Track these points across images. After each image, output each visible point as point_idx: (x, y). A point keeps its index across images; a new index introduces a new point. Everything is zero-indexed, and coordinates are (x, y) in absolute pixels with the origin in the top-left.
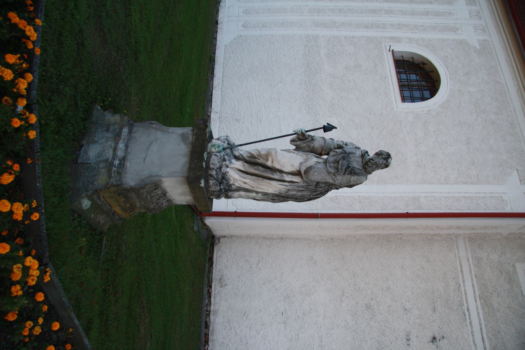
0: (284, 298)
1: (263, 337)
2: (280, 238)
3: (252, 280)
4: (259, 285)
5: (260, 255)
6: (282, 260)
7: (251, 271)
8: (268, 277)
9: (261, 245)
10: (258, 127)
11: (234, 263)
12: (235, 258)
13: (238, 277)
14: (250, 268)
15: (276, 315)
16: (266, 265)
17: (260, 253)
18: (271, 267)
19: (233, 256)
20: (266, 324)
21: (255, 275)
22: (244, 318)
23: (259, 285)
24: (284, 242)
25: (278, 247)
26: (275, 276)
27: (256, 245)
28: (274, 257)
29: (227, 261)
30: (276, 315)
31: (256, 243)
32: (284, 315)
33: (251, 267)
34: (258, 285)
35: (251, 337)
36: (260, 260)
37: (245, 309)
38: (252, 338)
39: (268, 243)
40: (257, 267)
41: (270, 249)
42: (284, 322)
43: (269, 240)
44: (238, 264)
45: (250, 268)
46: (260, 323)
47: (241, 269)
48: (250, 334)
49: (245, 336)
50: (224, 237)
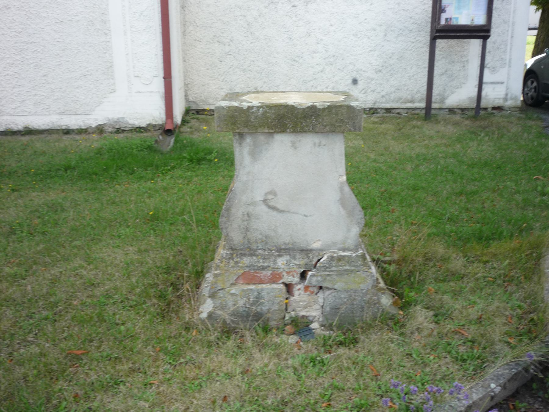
0: (272, 4)
1: (326, 34)
2: (182, 9)
3: (248, 52)
4: (254, 41)
5: (211, 41)
6: (217, 6)
7: (234, 53)
8: (243, 28)
9: (195, 40)
10: (4, 48)
11: (224, 79)
12: (217, 78)
13: (244, 72)
14: (230, 55)
15: (296, 16)
16: (225, 31)
17: (207, 41)
18: (227, 23)
19: (214, 81)
20: (308, 31)
21: (240, 48)
22: (301, 61)
23: (254, 41)
24: (189, 3)
25: (197, 13)
26: (241, 18)
27: (196, 47)
28: (212, 19)
29: (222, 89)
30: (296, 16)
31: (193, 47)
32: (296, 4)
33: (229, 53)
34: (255, 43)
35: (326, 50)
36: (218, 41)
37: (288, 61)
38: (327, 49)
39: (192, 29)
40: (229, 45)
41: (201, 26)
42: (305, 4)
43: (186, 27)
44: (226, 73)
45: (230, 55)
46: (307, 38)
47: (232, 69)
48: (322, 52)
49: (325, 59)
50: (186, 96)
